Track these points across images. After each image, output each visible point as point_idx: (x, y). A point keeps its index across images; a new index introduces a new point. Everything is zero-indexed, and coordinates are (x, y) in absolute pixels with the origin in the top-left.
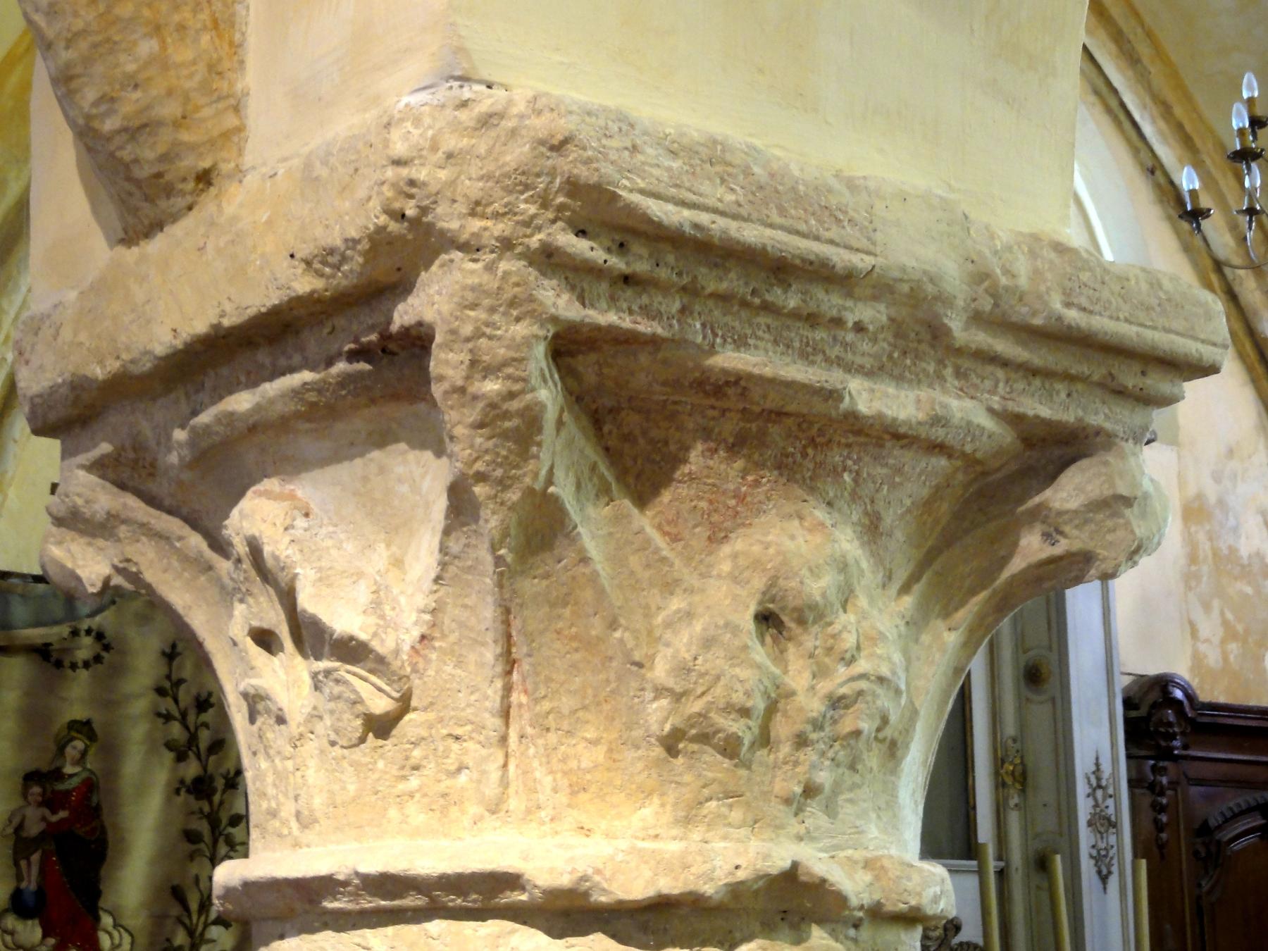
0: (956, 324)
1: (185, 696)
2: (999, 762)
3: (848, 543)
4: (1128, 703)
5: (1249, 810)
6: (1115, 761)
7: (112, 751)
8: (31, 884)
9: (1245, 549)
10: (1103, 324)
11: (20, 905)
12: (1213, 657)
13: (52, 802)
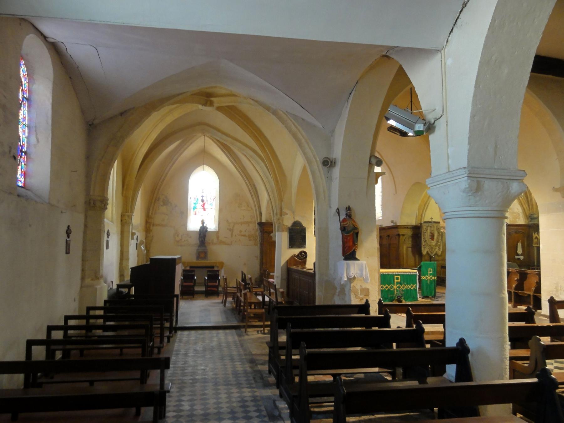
7: (434, 231)
8: (431, 237)
11: (430, 238)
12: (511, 220)
13: (431, 234)
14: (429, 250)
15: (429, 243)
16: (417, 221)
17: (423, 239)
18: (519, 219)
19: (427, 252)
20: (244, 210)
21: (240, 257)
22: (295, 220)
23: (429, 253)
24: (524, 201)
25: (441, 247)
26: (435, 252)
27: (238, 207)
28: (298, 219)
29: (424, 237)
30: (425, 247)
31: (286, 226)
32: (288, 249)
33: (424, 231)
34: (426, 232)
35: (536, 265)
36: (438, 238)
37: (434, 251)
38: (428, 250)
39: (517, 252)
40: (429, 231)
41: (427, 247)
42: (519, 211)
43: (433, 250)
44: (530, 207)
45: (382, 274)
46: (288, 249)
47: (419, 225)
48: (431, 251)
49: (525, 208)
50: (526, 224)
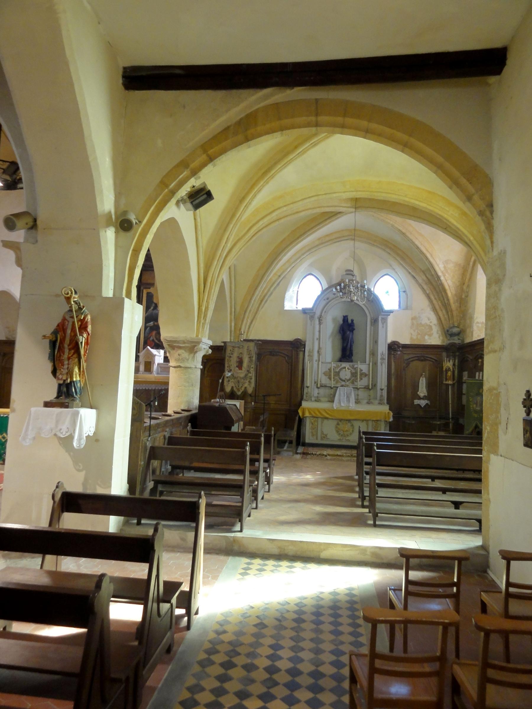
0: (186, 341)
1: (249, 350)
2: (370, 352)
3: (183, 351)
4: (389, 345)
5: (416, 357)
6: (386, 352)
8: (237, 365)
9: (423, 323)
10: (194, 341)
11: (237, 367)
12: (415, 337)
13: (239, 359)
14: (235, 384)
15: (235, 375)
16: (232, 338)
17: (228, 367)
18: (430, 335)
19: (232, 387)
23: (235, 389)
24: (440, 304)
25: (253, 381)
26: (243, 389)
29: (228, 364)
30: (229, 381)
33: (229, 356)
34: (231, 355)
35: (450, 417)
36: (249, 367)
37: (242, 387)
38: (233, 385)
39: (418, 393)
40: (235, 355)
41: (233, 380)
42: (431, 322)
43: (240, 386)
44: (449, 313)
47: (223, 344)
48: (237, 386)
49: (441, 316)
50: (444, 344)
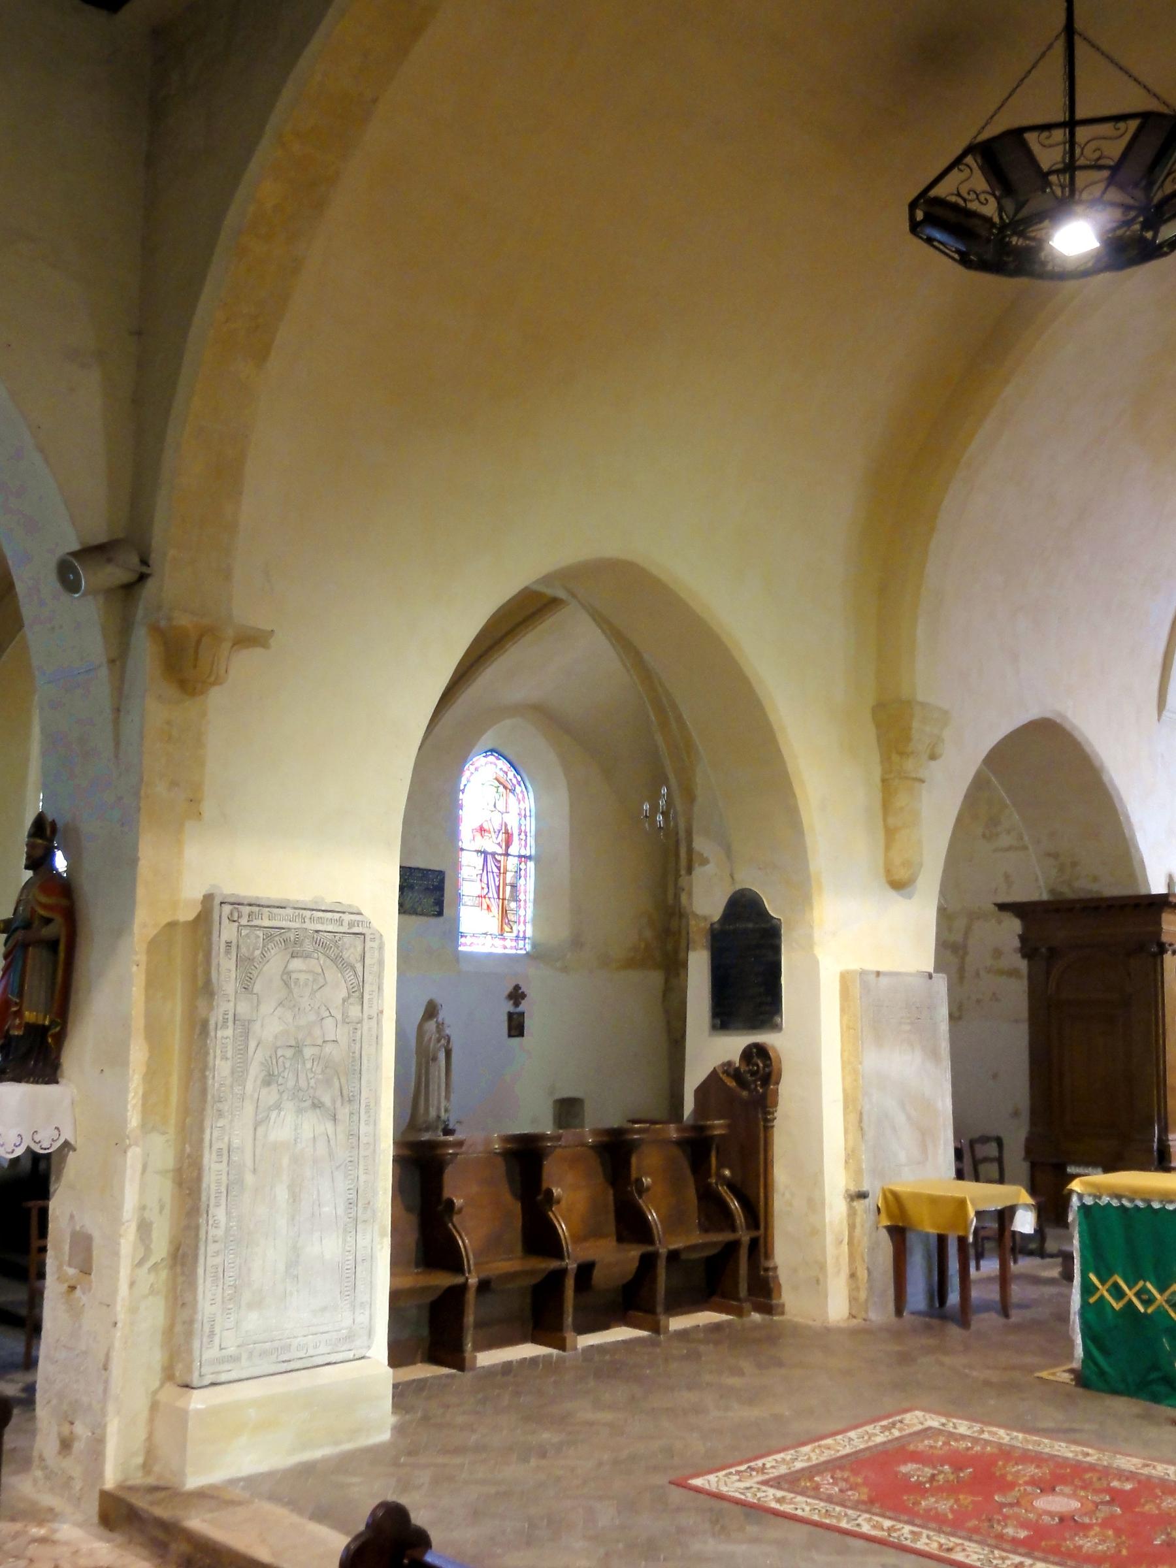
20: (1010, 848)
21: (995, 1076)
22: (738, 887)
27: (984, 836)
28: (749, 880)
31: (705, 918)
32: (710, 1035)
45: (1141, 1204)
46: (710, 1035)
